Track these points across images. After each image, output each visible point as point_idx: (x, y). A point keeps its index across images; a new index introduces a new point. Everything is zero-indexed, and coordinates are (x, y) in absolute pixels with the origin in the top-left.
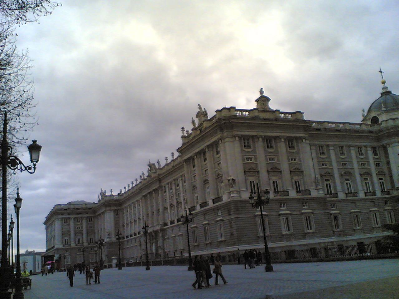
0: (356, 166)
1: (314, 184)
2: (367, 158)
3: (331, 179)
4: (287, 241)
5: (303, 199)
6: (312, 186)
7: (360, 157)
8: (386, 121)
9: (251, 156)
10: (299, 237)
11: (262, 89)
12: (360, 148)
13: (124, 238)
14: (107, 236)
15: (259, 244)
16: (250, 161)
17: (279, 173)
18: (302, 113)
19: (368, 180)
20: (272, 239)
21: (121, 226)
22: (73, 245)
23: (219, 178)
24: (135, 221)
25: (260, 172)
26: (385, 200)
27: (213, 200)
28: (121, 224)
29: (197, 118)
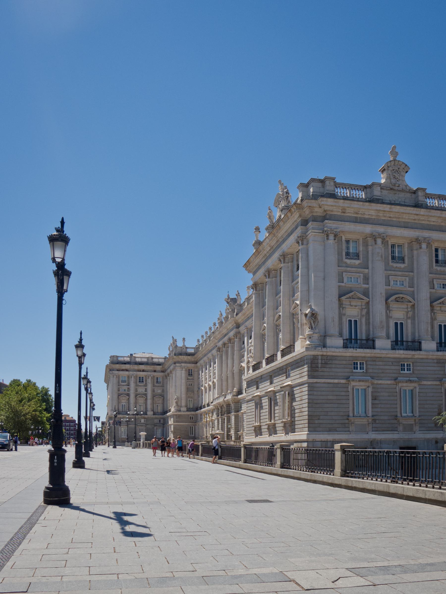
15: (349, 433)
20: (374, 425)
25: (370, 303)
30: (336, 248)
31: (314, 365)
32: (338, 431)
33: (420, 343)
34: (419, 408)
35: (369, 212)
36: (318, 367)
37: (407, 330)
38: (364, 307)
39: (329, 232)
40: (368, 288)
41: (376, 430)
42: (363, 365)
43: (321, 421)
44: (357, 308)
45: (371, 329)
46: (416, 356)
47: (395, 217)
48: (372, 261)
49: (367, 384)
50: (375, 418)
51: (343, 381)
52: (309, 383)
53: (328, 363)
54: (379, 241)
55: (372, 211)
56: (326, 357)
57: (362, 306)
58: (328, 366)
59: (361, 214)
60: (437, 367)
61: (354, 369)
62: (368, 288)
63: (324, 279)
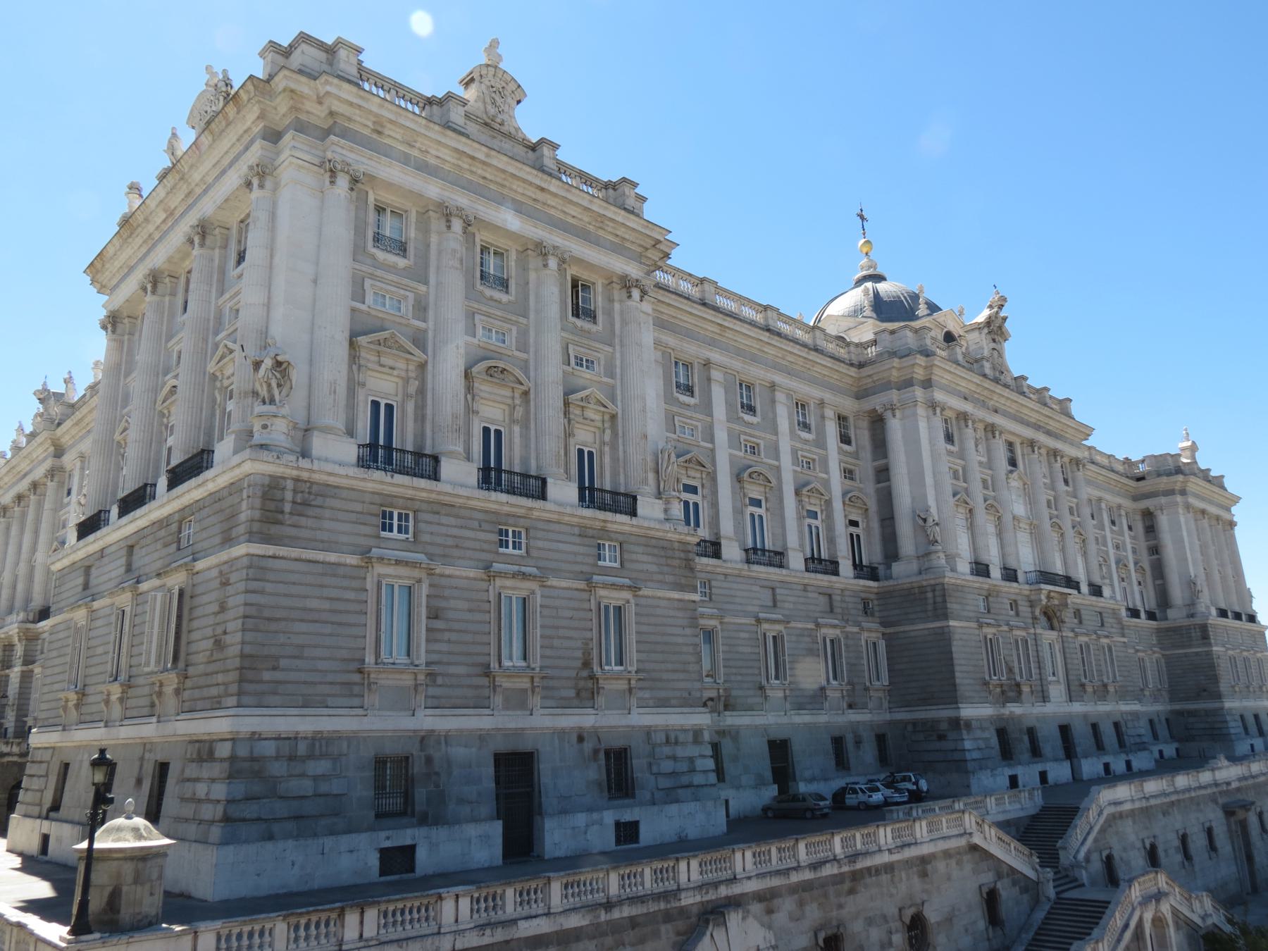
2: (821, 443)
3: (703, 486)
4: (508, 705)
7: (800, 433)
8: (893, 332)
10: (565, 693)
11: (494, 44)
12: (801, 406)
15: (360, 712)
17: (517, 395)
18: (644, 199)
19: (816, 518)
20: (432, 691)
25: (430, 367)
26: (863, 595)
29: (193, 127)
30: (353, 214)
31: (271, 506)
32: (329, 704)
33: (544, 481)
34: (542, 647)
35: (438, 150)
36: (282, 512)
37: (511, 449)
38: (412, 375)
39: (339, 167)
40: (425, 331)
41: (436, 704)
42: (407, 520)
43: (278, 675)
44: (395, 373)
46: (536, 514)
47: (496, 183)
48: (438, 268)
49: (417, 573)
50: (435, 668)
51: (352, 560)
52: (253, 555)
53: (313, 503)
54: (457, 225)
55: (446, 151)
56: (308, 484)
57: (407, 370)
58: (310, 512)
59: (420, 149)
60: (579, 545)
61: (384, 529)
63: (315, 281)
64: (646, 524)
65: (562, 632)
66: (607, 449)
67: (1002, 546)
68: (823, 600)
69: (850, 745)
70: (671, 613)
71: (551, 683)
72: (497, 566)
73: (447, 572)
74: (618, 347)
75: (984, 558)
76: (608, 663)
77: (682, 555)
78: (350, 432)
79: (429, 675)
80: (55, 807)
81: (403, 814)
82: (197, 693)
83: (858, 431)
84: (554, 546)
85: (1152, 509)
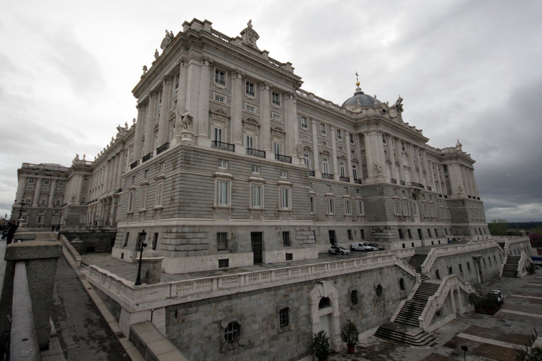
0: (334, 147)
1: (296, 151)
5: (282, 166)
6: (294, 153)
9: (222, 94)
10: (271, 215)
13: (88, 204)
14: (70, 199)
15: (213, 219)
16: (221, 101)
17: (257, 127)
21: (89, 192)
22: (35, 205)
23: (172, 120)
24: (99, 187)
25: (232, 118)
27: (158, 149)
28: (89, 190)
37: (255, 143)
42: (226, 163)
43: (189, 208)
45: (231, 138)
50: (234, 207)
62: (230, 108)
64: (295, 166)
65: (270, 197)
66: (283, 143)
67: (400, 175)
68: (345, 189)
69: (353, 232)
70: (302, 192)
71: (267, 212)
72: (251, 178)
73: (237, 179)
74: (286, 113)
75: (395, 178)
76: (284, 206)
77: (305, 175)
78: (209, 137)
79: (232, 209)
80: (125, 245)
81: (225, 249)
82: (166, 213)
83: (356, 139)
84: (268, 172)
85: (446, 164)
